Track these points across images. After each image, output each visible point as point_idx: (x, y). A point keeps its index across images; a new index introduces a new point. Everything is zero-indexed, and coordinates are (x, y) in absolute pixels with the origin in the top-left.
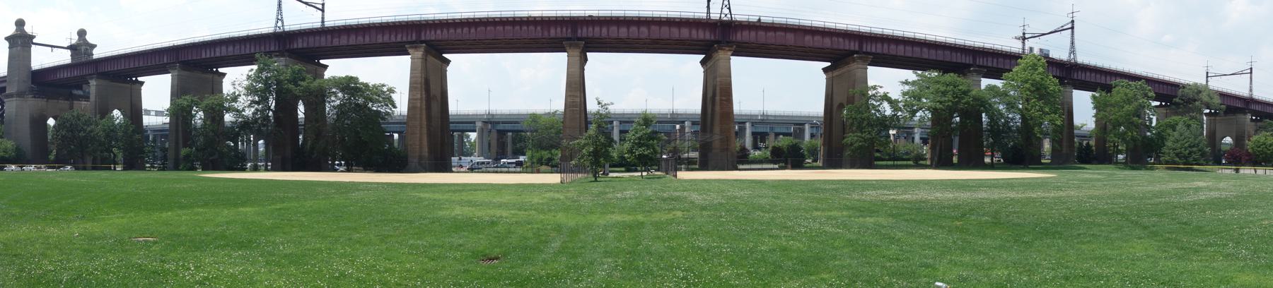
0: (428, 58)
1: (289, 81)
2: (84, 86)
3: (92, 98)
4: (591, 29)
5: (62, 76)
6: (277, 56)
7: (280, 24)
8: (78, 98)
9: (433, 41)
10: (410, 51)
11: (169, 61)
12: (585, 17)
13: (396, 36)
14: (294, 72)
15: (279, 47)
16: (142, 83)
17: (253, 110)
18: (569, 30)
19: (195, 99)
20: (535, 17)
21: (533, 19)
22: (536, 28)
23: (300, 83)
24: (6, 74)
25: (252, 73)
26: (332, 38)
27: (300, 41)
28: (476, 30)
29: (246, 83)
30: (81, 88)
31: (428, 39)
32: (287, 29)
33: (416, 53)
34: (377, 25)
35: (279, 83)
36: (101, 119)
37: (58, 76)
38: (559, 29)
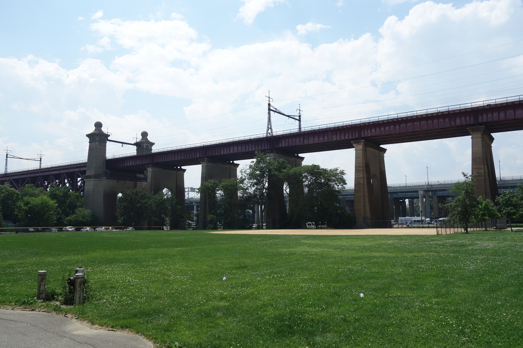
0: (367, 149)
1: (276, 170)
2: (145, 171)
3: (149, 180)
4: (490, 115)
5: (128, 164)
6: (268, 153)
7: (270, 131)
8: (141, 180)
9: (370, 137)
10: (354, 145)
11: (200, 156)
12: (484, 106)
13: (344, 136)
14: (279, 163)
15: (270, 146)
16: (185, 170)
17: (254, 189)
18: (472, 118)
19: (216, 182)
20: (443, 112)
21: (441, 114)
22: (444, 120)
23: (283, 170)
24: (86, 161)
25: (253, 164)
26: (304, 139)
27: (283, 142)
28: (400, 127)
29: (249, 170)
30: (143, 173)
31: (366, 136)
32: (274, 134)
33: (358, 146)
34: (332, 129)
35: (270, 171)
36: (154, 195)
37: (126, 164)
38: (463, 119)
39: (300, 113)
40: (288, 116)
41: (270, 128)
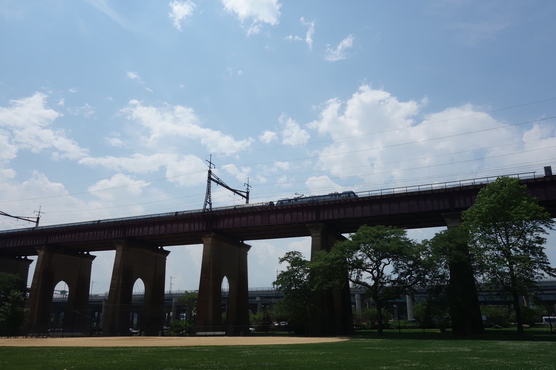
39: (248, 189)
40: (235, 191)
41: (208, 203)
